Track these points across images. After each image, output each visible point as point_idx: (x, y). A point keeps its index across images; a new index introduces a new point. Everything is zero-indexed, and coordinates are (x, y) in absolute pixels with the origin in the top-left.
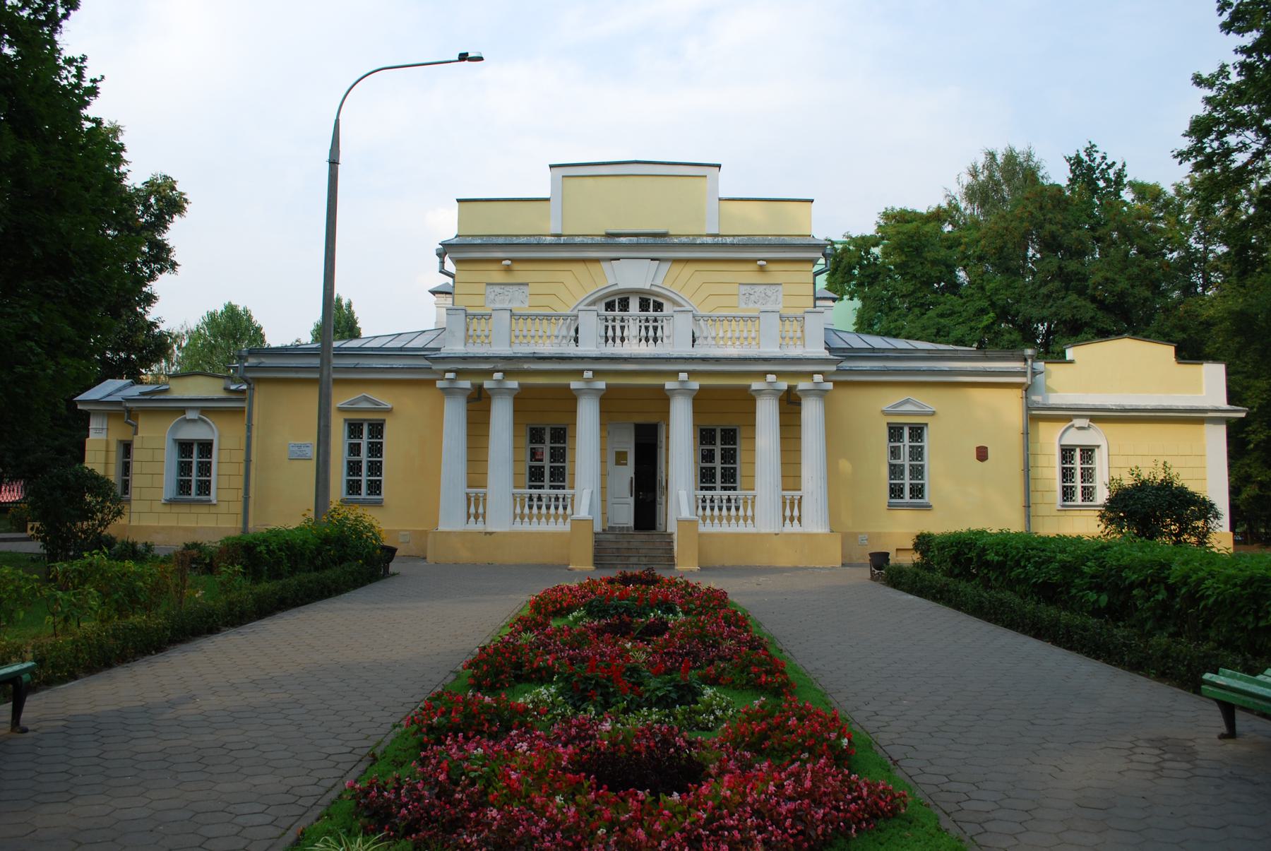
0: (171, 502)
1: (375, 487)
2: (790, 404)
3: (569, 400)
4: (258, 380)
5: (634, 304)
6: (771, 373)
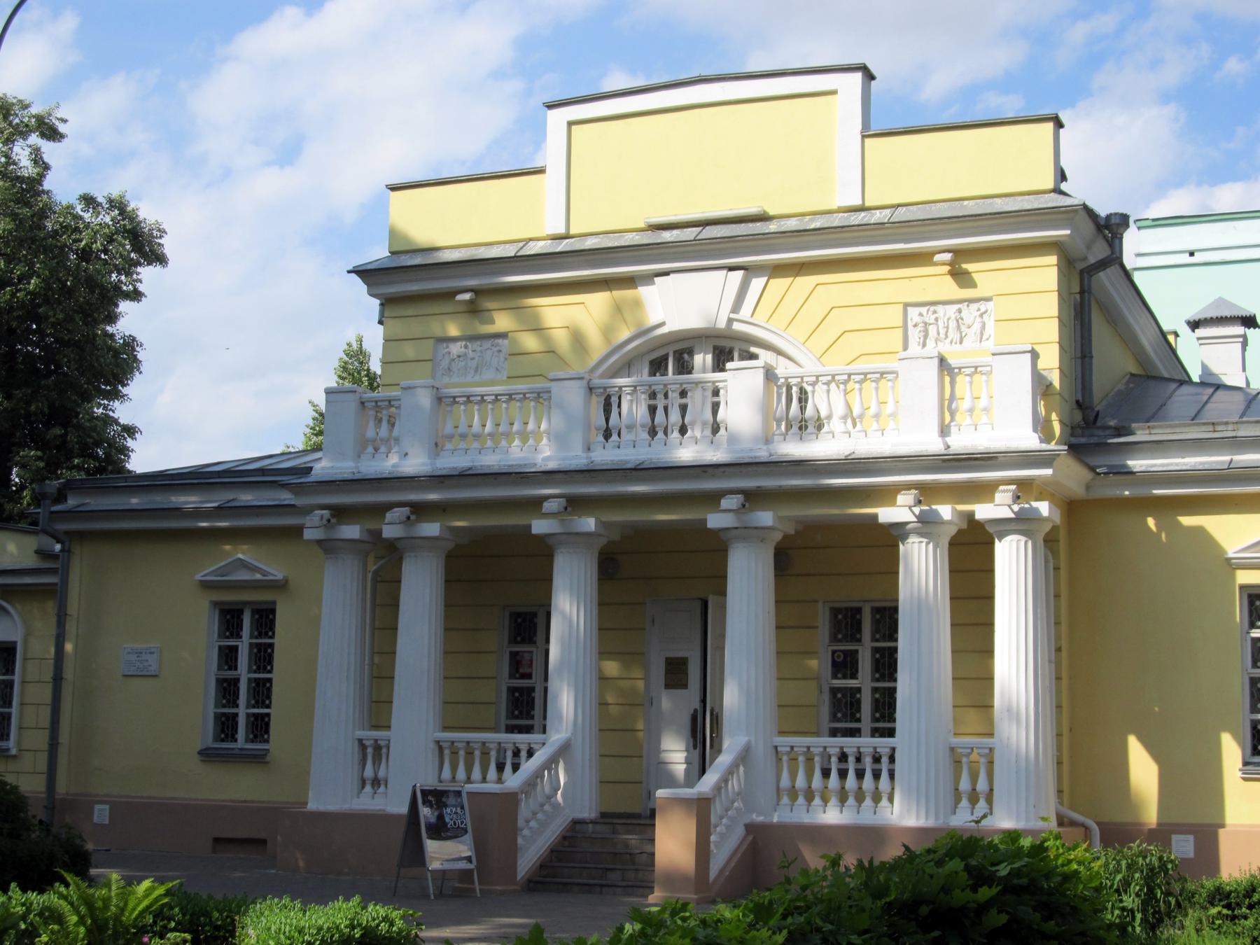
1: (260, 727)
2: (970, 554)
3: (537, 558)
4: (81, 536)
5: (702, 359)
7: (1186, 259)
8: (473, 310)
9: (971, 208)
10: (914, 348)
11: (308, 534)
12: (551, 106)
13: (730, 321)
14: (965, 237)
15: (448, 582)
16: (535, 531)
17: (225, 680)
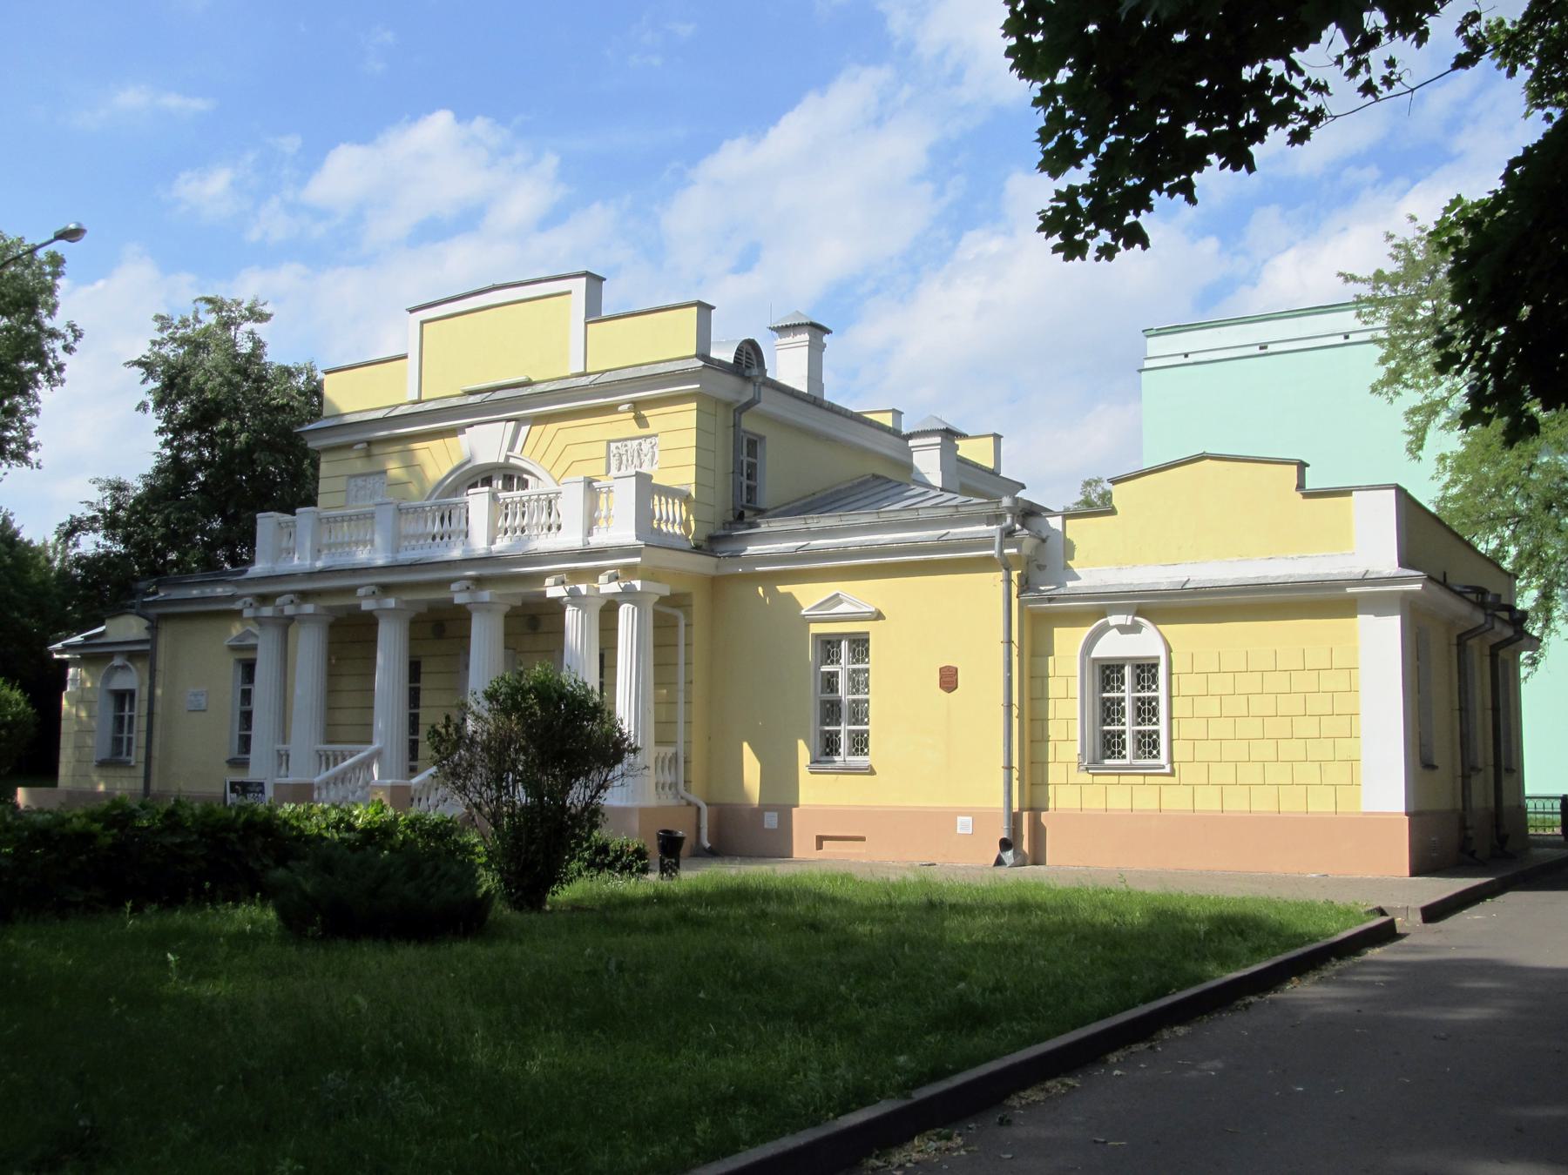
0: (102, 764)
7: (1182, 360)
8: (368, 455)
9: (645, 371)
10: (614, 472)
11: (247, 613)
12: (412, 311)
13: (507, 457)
14: (640, 392)
15: (331, 643)
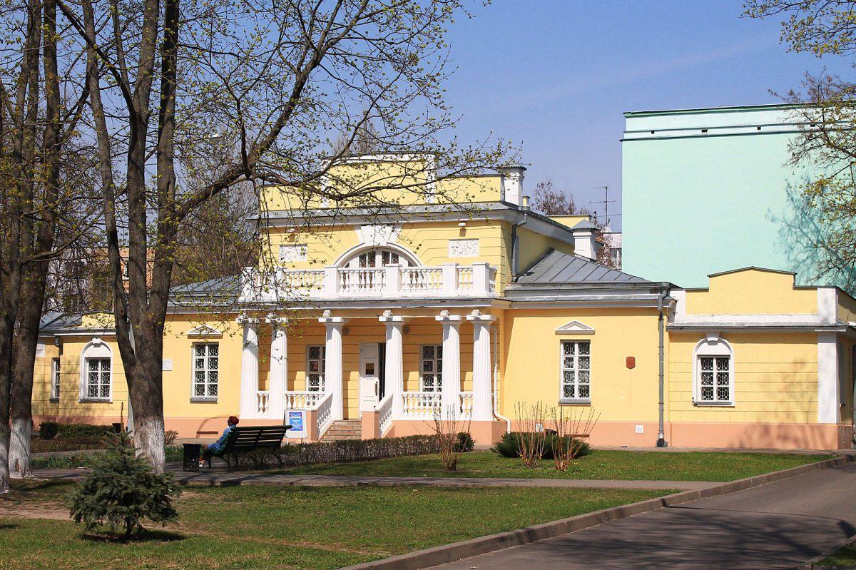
1: (213, 389)
5: (379, 258)
6: (445, 309)
16: (320, 321)
17: (198, 372)
